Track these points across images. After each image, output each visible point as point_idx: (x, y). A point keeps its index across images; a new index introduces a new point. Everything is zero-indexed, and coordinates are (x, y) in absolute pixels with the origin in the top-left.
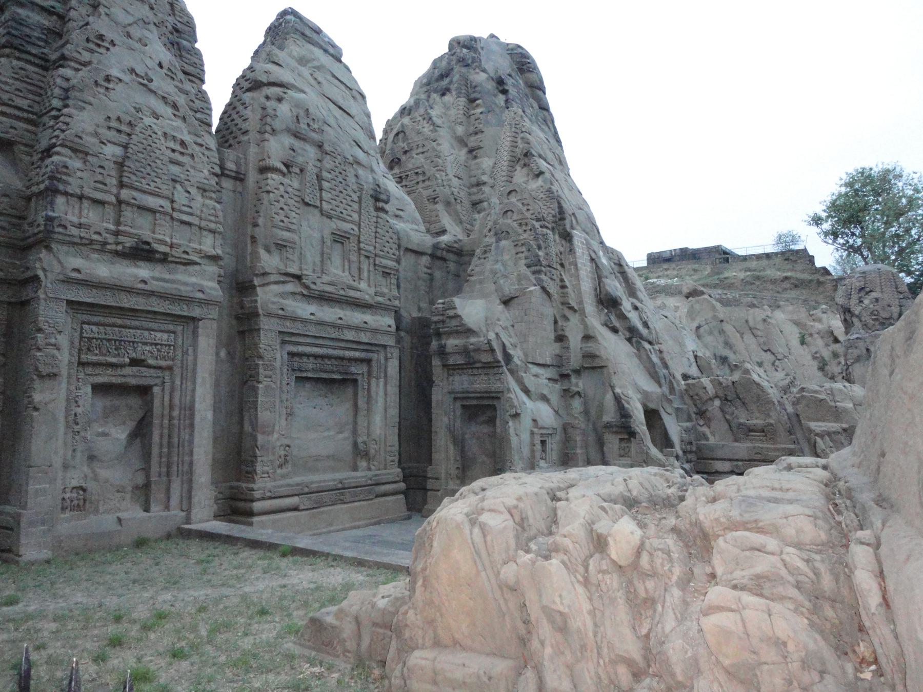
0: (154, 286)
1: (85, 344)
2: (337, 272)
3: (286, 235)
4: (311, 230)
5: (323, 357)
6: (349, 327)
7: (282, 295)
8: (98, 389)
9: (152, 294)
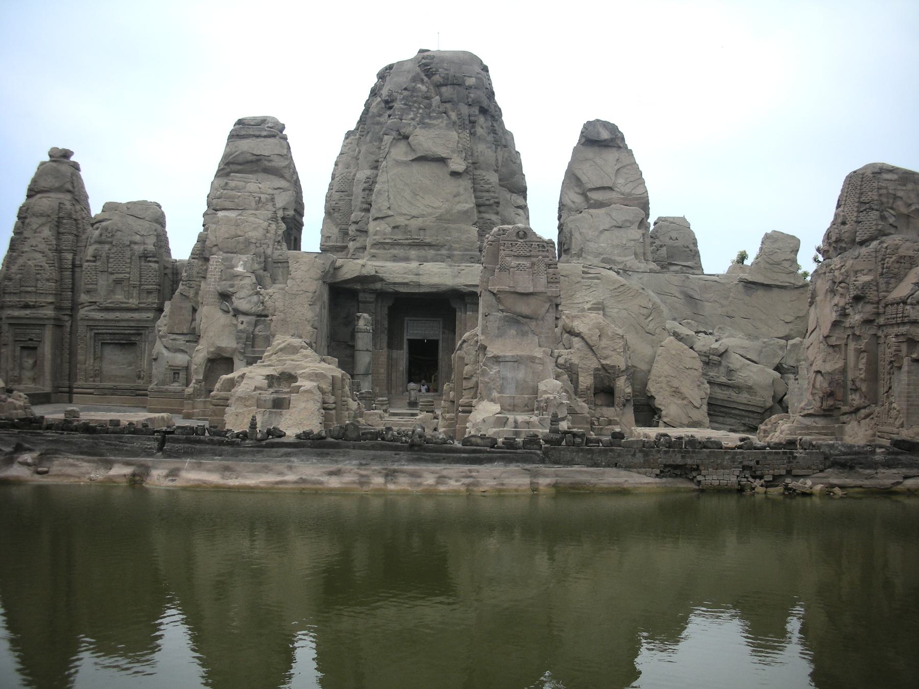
0: (32, 315)
2: (119, 297)
3: (90, 286)
4: (103, 282)
5: (115, 334)
6: (123, 320)
7: (89, 311)
8: (22, 348)
9: (30, 318)
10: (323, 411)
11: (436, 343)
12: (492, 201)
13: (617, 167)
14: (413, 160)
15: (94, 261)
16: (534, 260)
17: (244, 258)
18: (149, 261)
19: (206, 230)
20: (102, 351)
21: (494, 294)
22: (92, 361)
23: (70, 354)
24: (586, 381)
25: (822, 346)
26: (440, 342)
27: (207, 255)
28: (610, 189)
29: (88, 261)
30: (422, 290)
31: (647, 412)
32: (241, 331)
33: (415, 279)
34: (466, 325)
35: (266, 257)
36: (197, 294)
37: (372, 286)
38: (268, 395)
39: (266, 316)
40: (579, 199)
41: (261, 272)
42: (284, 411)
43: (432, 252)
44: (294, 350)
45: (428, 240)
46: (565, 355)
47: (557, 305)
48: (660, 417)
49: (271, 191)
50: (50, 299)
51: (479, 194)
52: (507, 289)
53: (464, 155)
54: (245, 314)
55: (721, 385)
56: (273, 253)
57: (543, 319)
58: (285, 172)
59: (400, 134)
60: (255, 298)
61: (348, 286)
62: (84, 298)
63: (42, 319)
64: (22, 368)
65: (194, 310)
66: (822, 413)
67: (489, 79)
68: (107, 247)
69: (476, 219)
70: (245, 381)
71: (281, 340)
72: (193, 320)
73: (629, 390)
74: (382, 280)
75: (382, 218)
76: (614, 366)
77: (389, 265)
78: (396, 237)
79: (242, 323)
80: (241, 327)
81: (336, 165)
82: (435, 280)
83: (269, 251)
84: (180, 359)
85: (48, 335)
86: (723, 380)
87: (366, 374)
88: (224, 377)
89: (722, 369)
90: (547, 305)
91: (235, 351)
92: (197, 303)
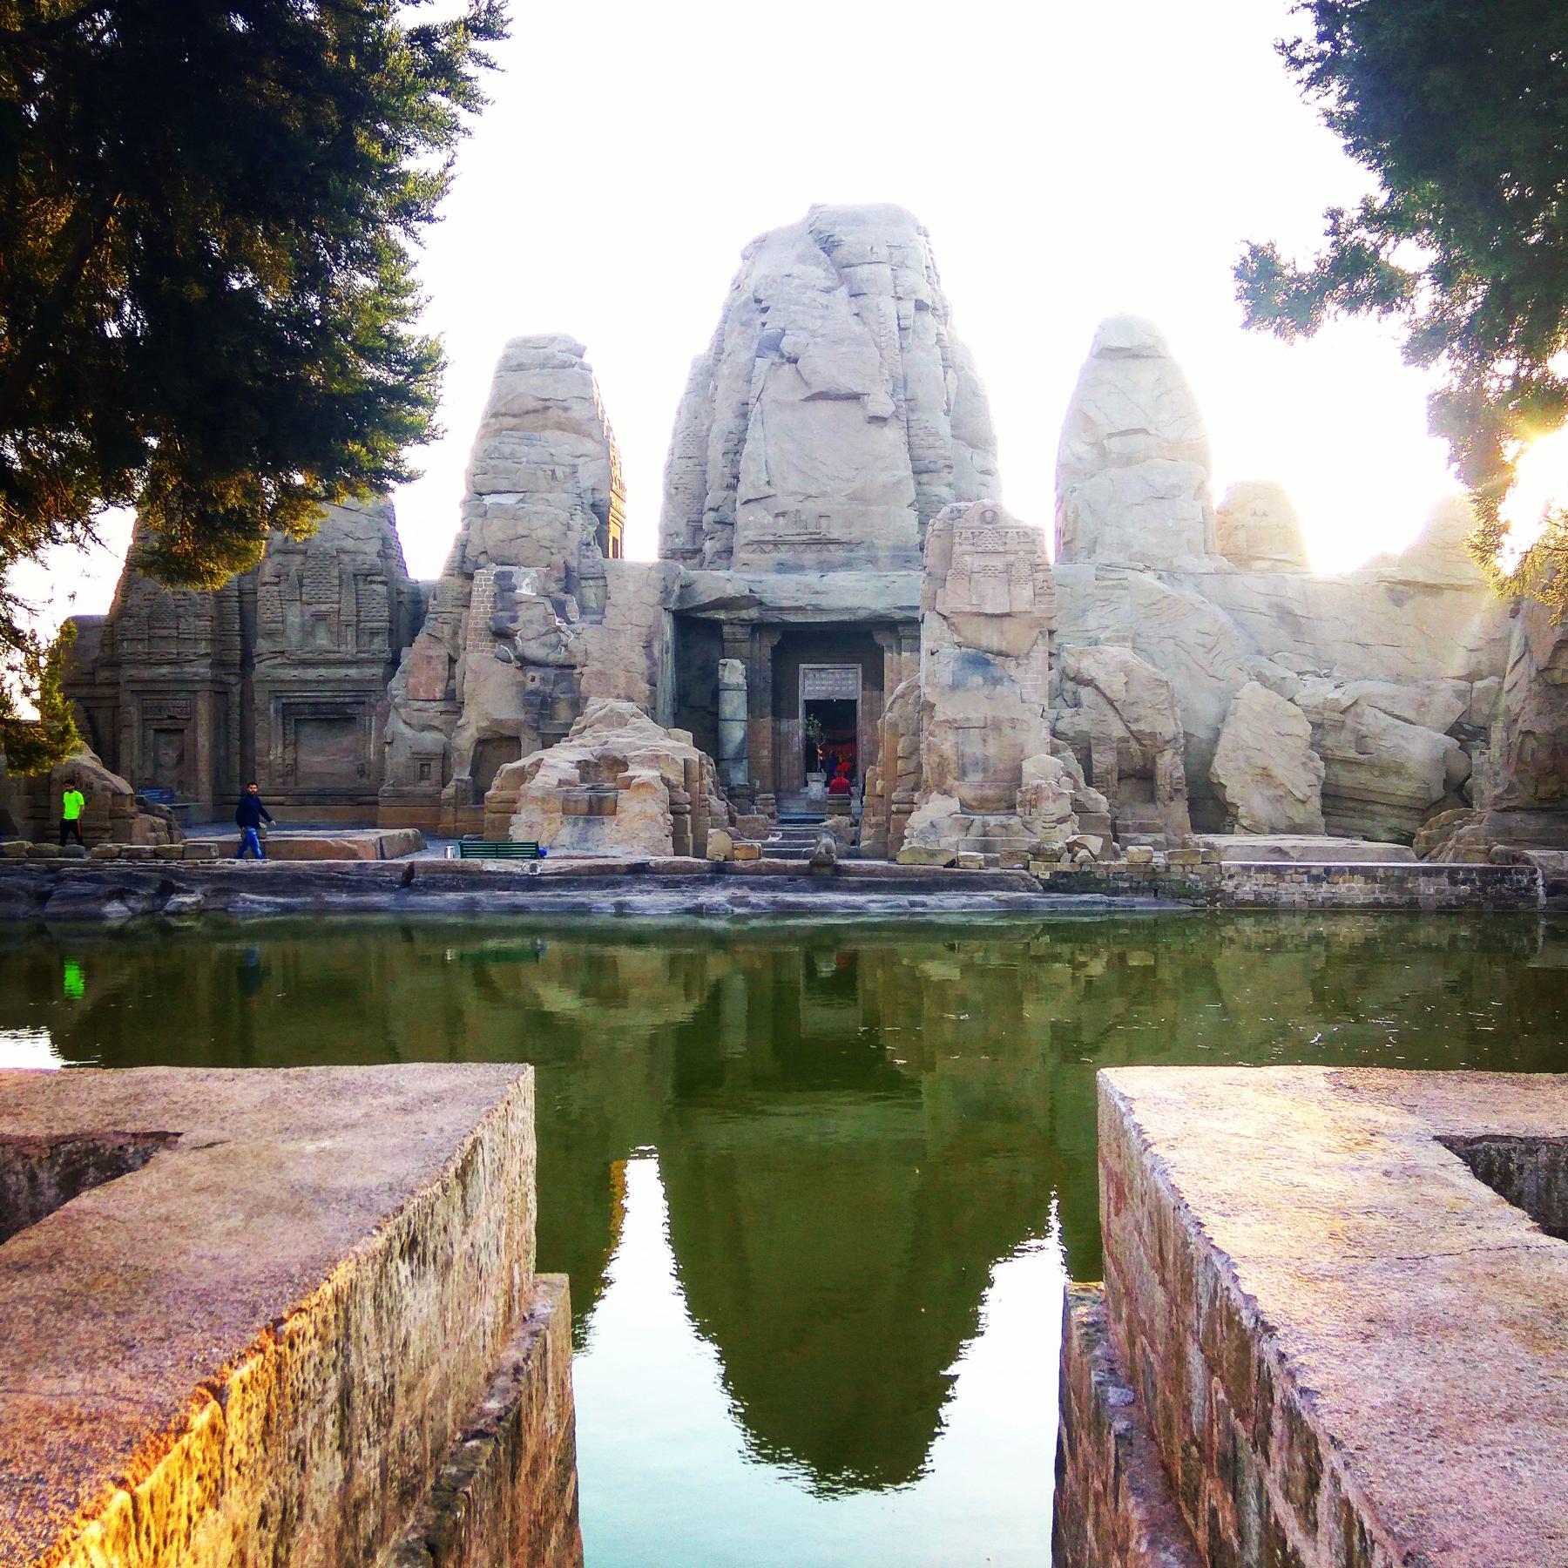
0: (171, 677)
1: (145, 710)
2: (323, 640)
4: (294, 616)
7: (274, 667)
8: (157, 731)
10: (670, 817)
12: (941, 463)
13: (1156, 393)
14: (808, 399)
15: (276, 584)
16: (1011, 558)
17: (533, 572)
18: (371, 582)
19: (467, 527)
20: (296, 733)
21: (945, 618)
22: (280, 750)
23: (242, 738)
24: (1103, 760)
25: (1535, 687)
27: (469, 567)
28: (1144, 431)
29: (265, 584)
30: (824, 618)
31: (1210, 808)
32: (534, 693)
33: (815, 600)
35: (568, 570)
36: (455, 633)
37: (744, 614)
38: (582, 793)
39: (573, 667)
41: (562, 596)
42: (606, 819)
43: (839, 554)
44: (620, 720)
45: (835, 534)
46: (1070, 721)
47: (1051, 633)
48: (1236, 817)
49: (570, 460)
50: (203, 648)
51: (920, 452)
52: (968, 609)
54: (537, 664)
55: (1346, 762)
56: (580, 563)
57: (1027, 655)
58: (592, 429)
59: (782, 356)
60: (553, 638)
61: (704, 615)
62: (262, 645)
63: (193, 682)
64: (158, 765)
65: (452, 661)
66: (1536, 804)
68: (298, 559)
70: (542, 771)
71: (596, 706)
72: (451, 677)
73: (1180, 772)
74: (760, 603)
76: (1153, 735)
77: (772, 578)
79: (533, 680)
80: (531, 686)
81: (679, 413)
82: (850, 601)
83: (574, 563)
84: (431, 740)
85: (203, 708)
86: (1352, 754)
88: (509, 766)
89: (1345, 736)
90: (1035, 633)
91: (520, 724)
92: (456, 648)
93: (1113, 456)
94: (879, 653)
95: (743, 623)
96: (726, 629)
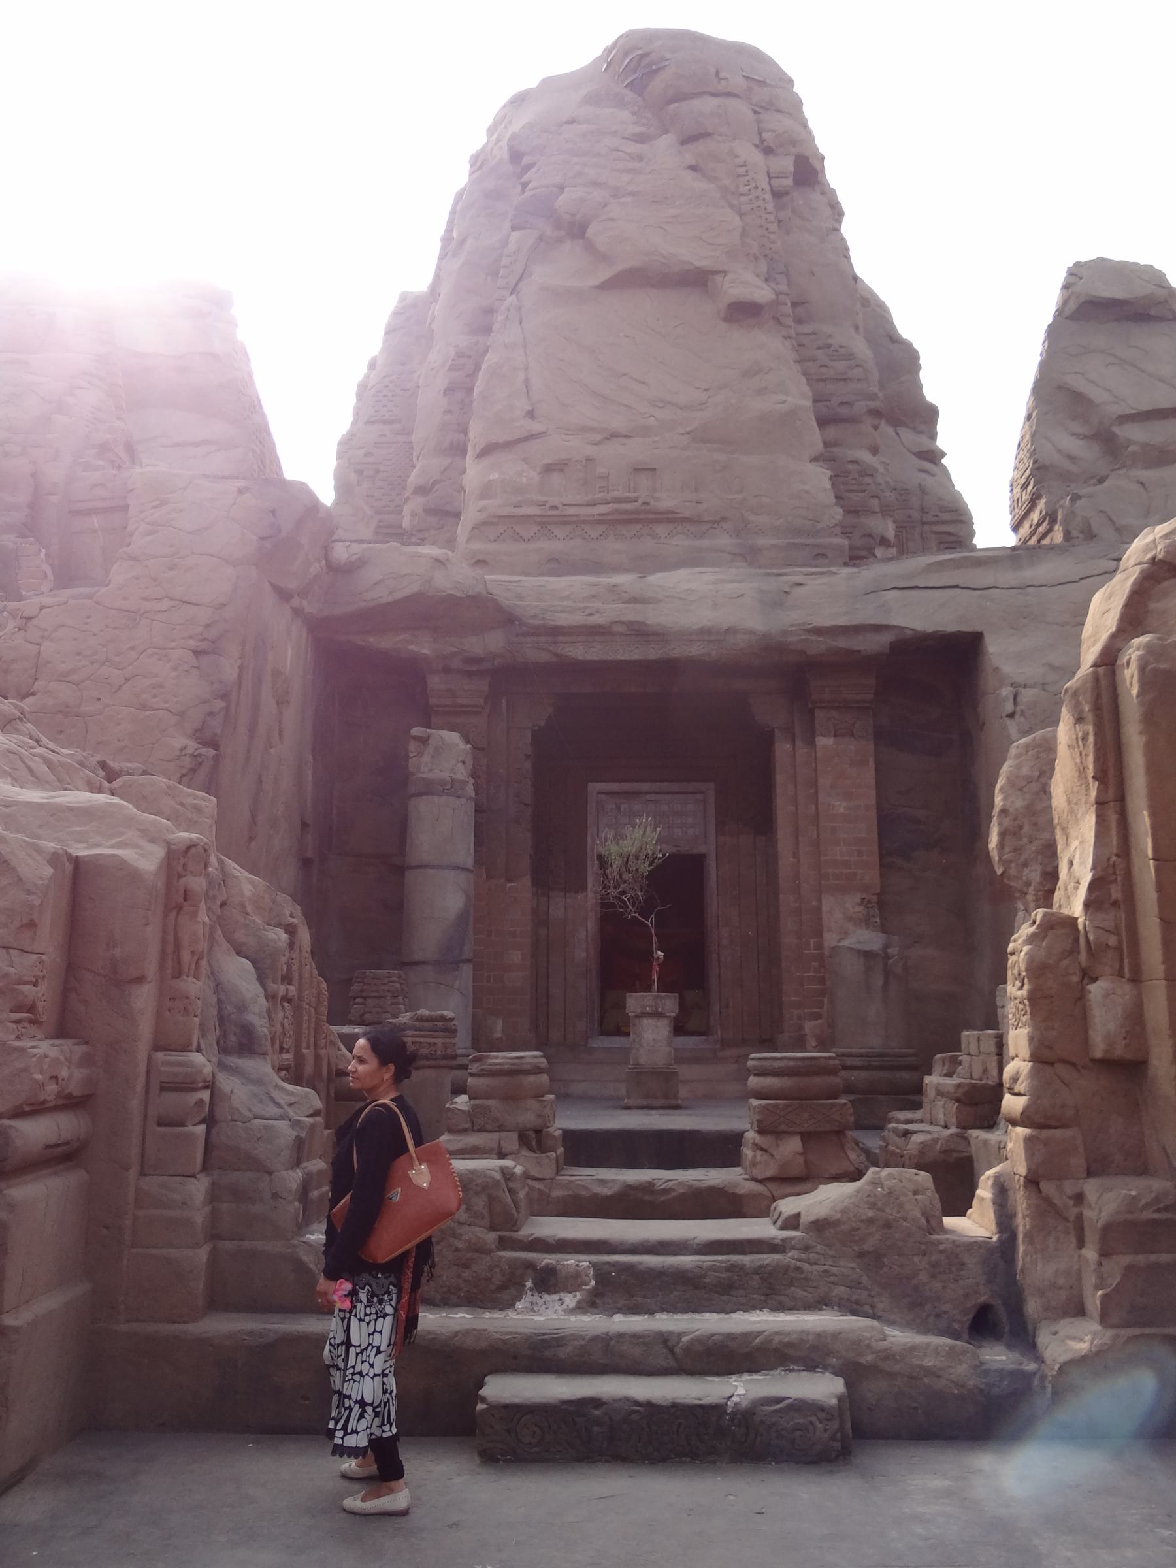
11: (697, 861)
12: (861, 406)
26: (711, 863)
33: (631, 614)
34: (814, 784)
37: (476, 645)
40: (1087, 452)
43: (681, 542)
45: (666, 502)
53: (763, 267)
61: (385, 642)
67: (805, 126)
69: (820, 447)
74: (508, 619)
75: (507, 445)
78: (555, 500)
82: (702, 617)
87: (448, 962)
93: (1132, 448)
94: (766, 741)
95: (474, 667)
96: (435, 682)
